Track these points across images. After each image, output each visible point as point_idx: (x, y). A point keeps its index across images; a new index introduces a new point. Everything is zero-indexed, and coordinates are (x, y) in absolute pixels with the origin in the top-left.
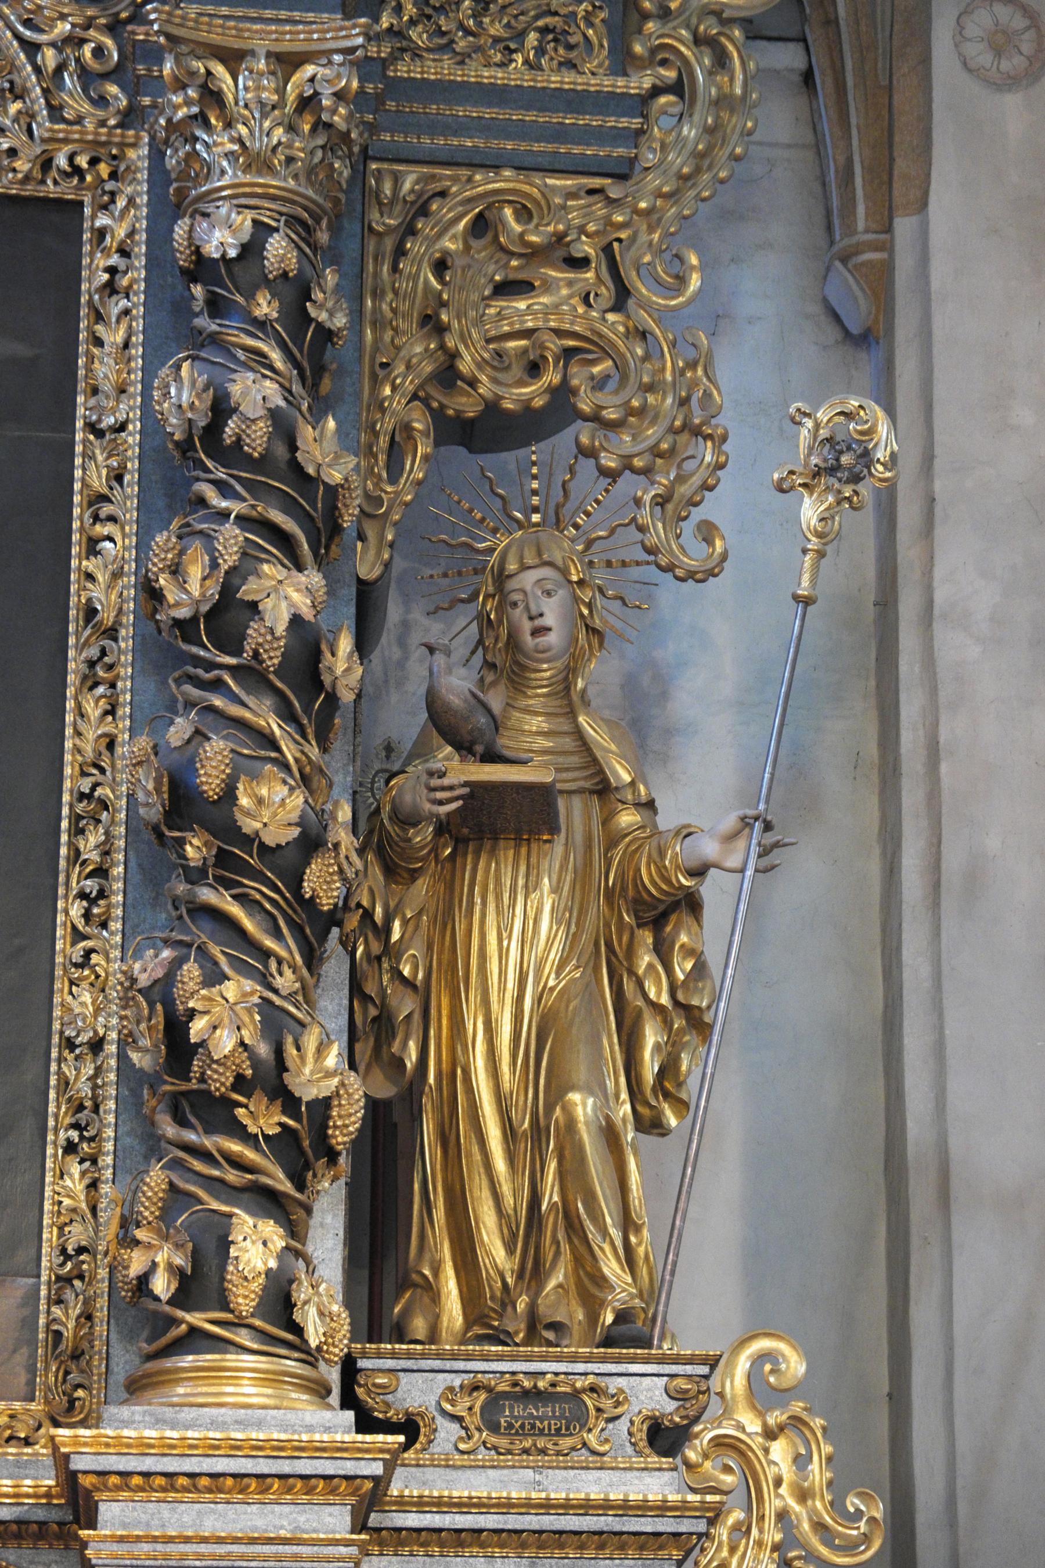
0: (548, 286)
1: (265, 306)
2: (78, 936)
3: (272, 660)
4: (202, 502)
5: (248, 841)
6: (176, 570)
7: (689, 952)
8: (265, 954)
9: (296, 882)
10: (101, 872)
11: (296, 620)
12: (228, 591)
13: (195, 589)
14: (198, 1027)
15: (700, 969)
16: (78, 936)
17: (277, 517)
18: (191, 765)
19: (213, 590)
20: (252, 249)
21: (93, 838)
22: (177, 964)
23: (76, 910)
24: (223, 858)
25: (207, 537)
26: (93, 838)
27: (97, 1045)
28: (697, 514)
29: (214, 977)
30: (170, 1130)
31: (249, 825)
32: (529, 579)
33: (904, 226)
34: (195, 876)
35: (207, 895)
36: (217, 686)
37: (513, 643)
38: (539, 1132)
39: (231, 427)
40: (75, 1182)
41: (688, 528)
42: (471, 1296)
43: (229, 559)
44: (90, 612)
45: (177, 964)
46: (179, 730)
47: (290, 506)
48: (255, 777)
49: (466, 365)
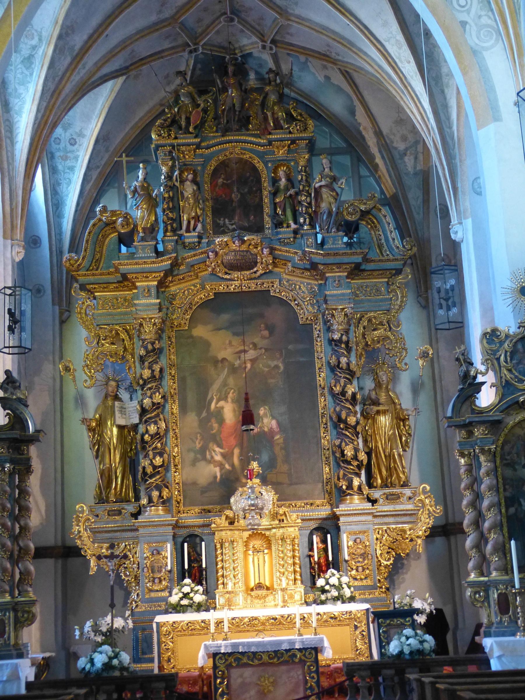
0: (380, 329)
1: (343, 346)
2: (324, 433)
3: (350, 398)
4: (337, 374)
5: (350, 425)
6: (335, 386)
7: (408, 425)
8: (353, 440)
9: (356, 429)
10: (326, 424)
11: (352, 392)
12: (343, 389)
13: (338, 388)
14: (346, 452)
15: (410, 427)
16: (324, 433)
17: (348, 376)
18: (341, 413)
19: (341, 389)
20: (341, 338)
21: (324, 420)
22: (341, 442)
23: (323, 430)
24: (346, 427)
25: (339, 381)
26: (324, 420)
27: (328, 449)
28: (404, 361)
29: (347, 444)
30: (342, 465)
31: (349, 423)
32: (381, 373)
33: (429, 291)
34: (342, 429)
35: (344, 432)
36: (342, 402)
37: (379, 382)
38: (390, 455)
39: (341, 365)
40: (327, 469)
41: (403, 363)
42: (382, 478)
43: (342, 385)
44: (320, 386)
45: (341, 442)
46: (338, 409)
47: (349, 374)
48: (349, 416)
49: (369, 343)
